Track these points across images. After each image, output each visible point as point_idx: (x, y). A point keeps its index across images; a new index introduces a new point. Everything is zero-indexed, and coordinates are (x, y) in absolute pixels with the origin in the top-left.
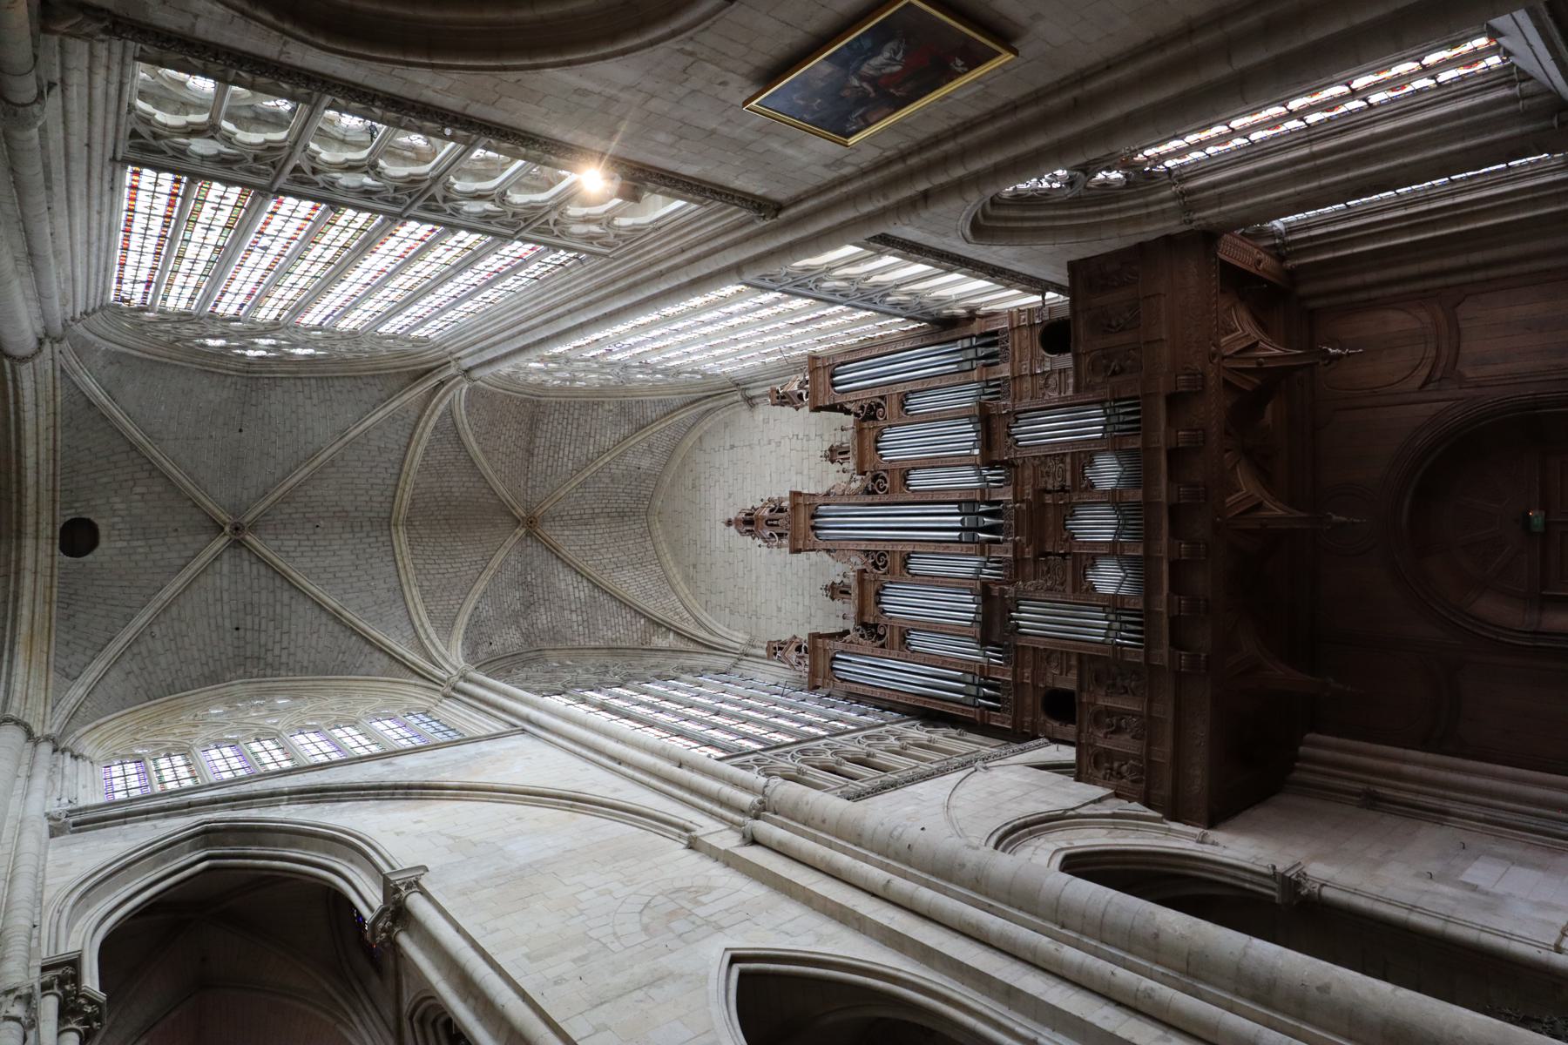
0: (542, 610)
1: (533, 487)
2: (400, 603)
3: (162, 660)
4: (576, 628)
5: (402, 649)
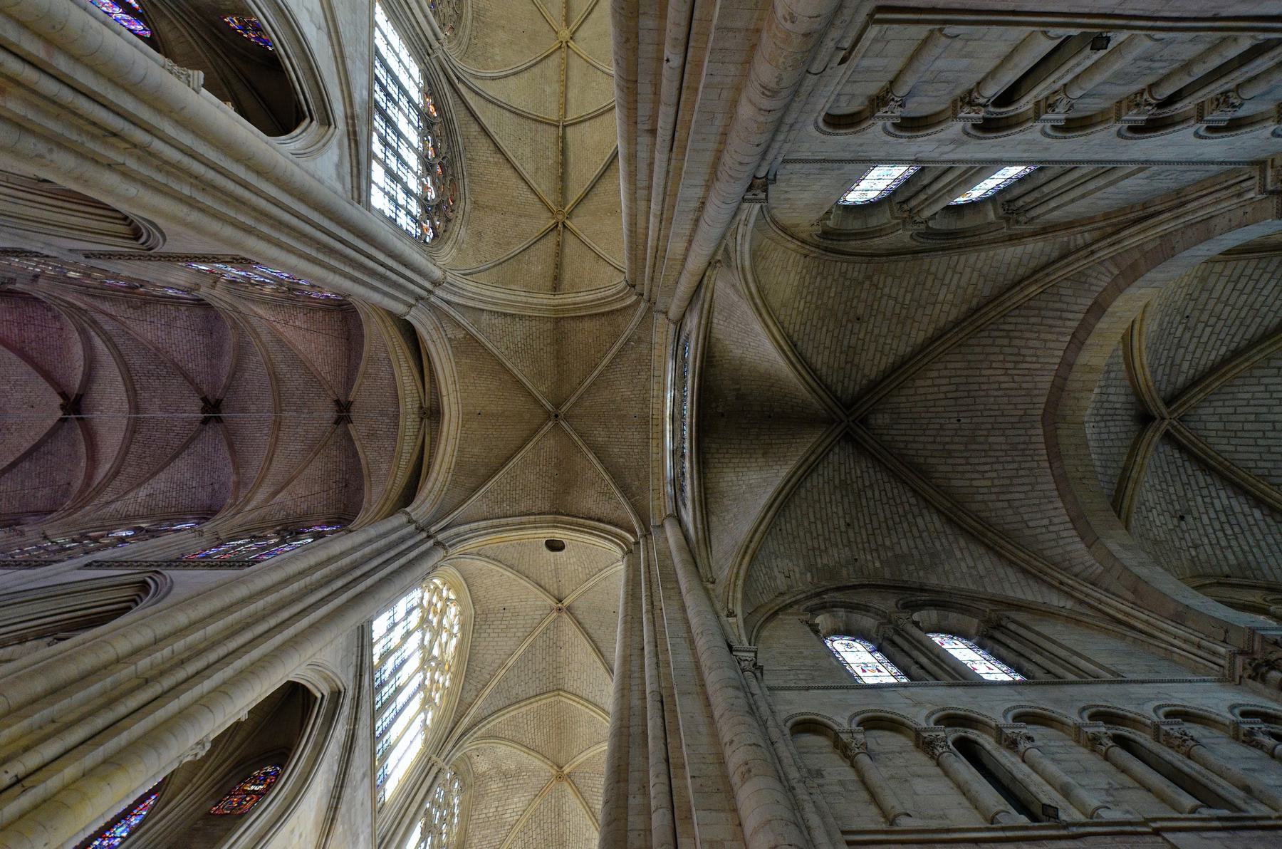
0: (501, 784)
1: (585, 778)
2: (507, 702)
4: (485, 811)
5: (473, 712)
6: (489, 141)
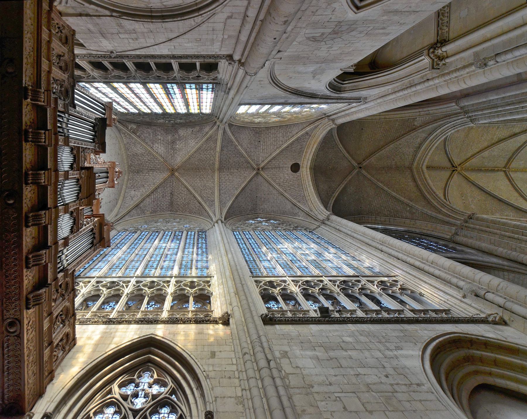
3: (281, 135)
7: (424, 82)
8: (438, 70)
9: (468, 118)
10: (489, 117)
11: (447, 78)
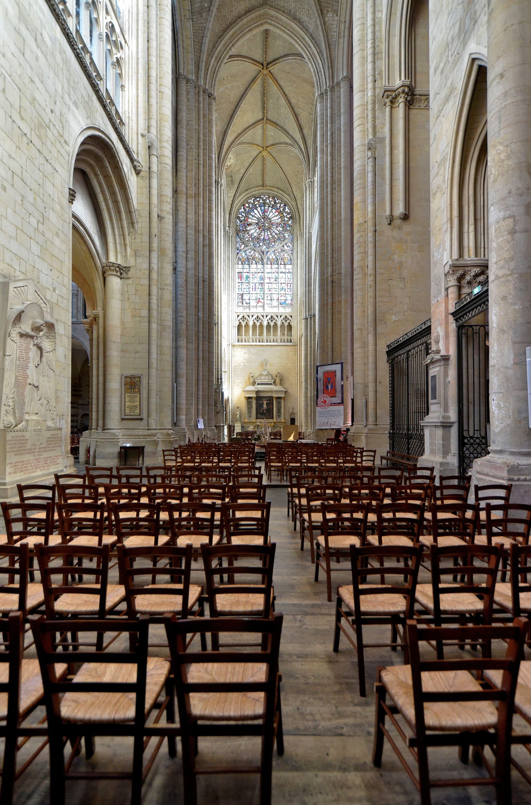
6: (300, 122)
7: (374, 76)
8: (381, 96)
9: (326, 90)
10: (322, 114)
11: (370, 107)
